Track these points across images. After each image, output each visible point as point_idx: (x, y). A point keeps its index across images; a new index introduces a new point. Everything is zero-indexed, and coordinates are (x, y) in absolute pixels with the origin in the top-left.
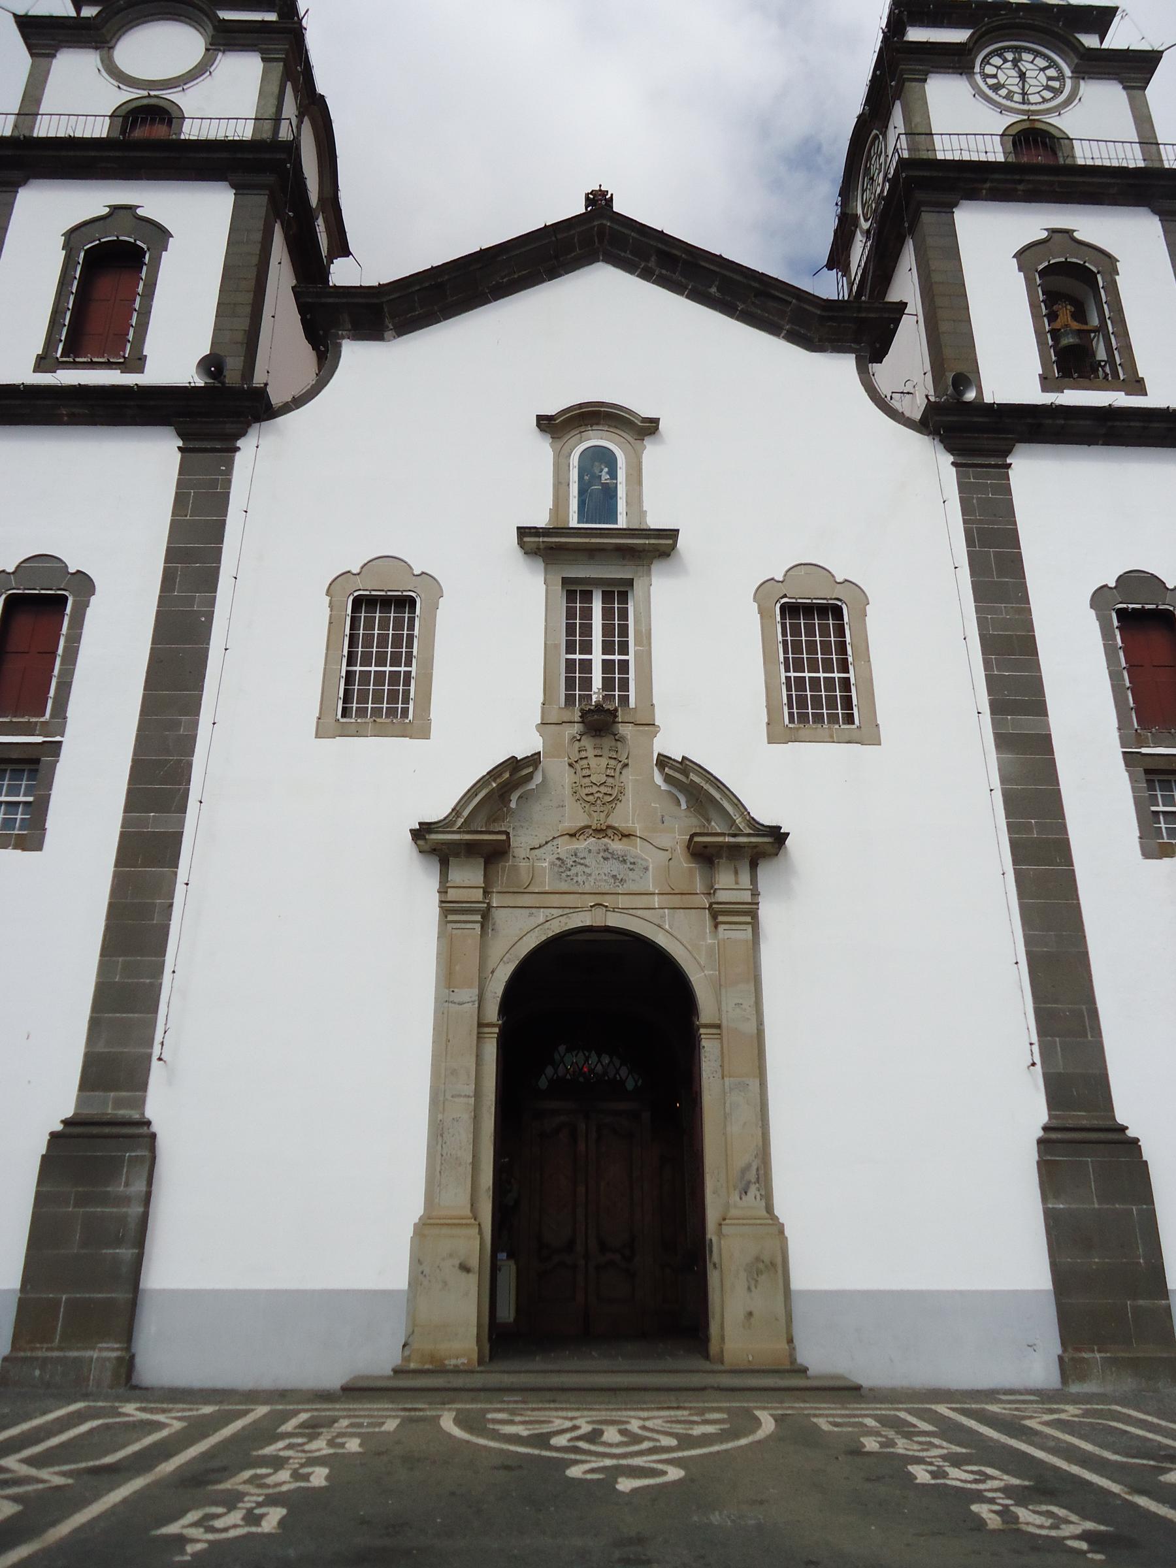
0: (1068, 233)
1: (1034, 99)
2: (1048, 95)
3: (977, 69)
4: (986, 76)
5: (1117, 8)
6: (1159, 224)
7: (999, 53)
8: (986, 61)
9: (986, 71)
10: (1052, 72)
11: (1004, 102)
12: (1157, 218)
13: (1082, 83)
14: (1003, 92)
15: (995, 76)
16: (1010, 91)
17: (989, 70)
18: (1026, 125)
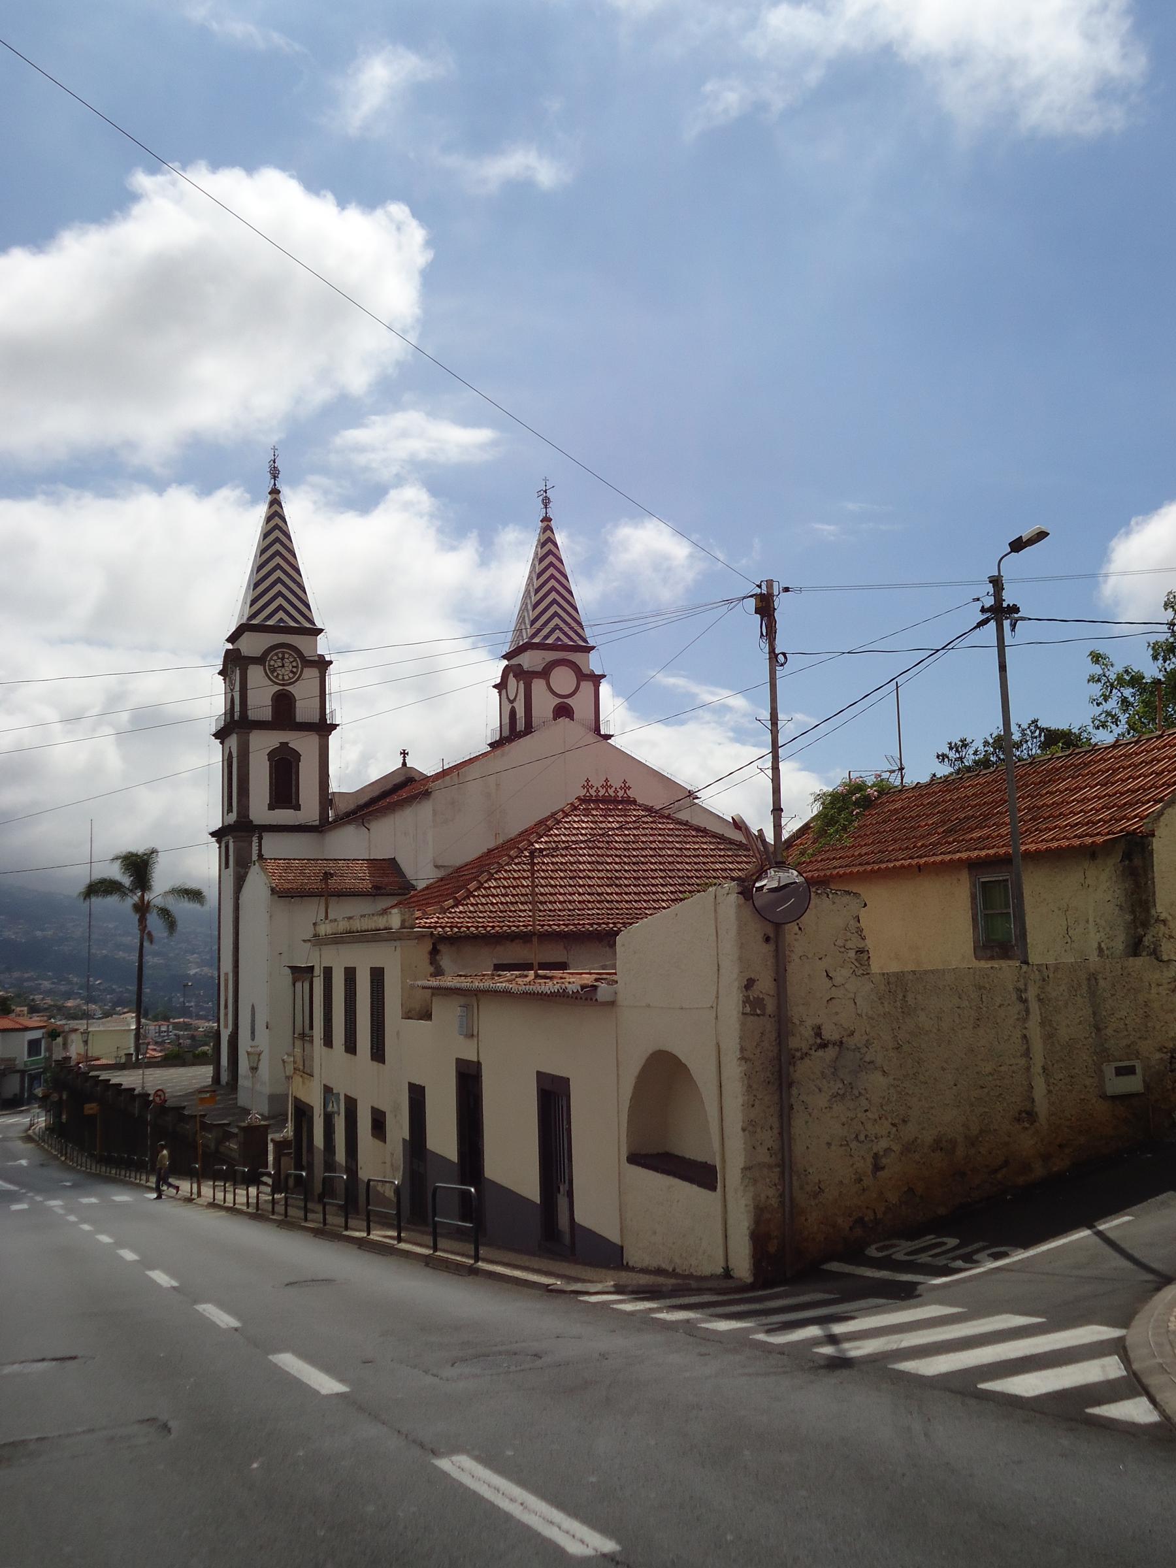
0: (287, 743)
1: (286, 678)
2: (291, 675)
3: (267, 664)
4: (271, 666)
5: (323, 630)
6: (318, 740)
7: (276, 654)
8: (271, 659)
9: (271, 664)
10: (294, 664)
11: (274, 679)
12: (317, 737)
13: (306, 670)
14: (275, 674)
15: (274, 666)
16: (278, 674)
17: (272, 663)
18: (281, 692)
